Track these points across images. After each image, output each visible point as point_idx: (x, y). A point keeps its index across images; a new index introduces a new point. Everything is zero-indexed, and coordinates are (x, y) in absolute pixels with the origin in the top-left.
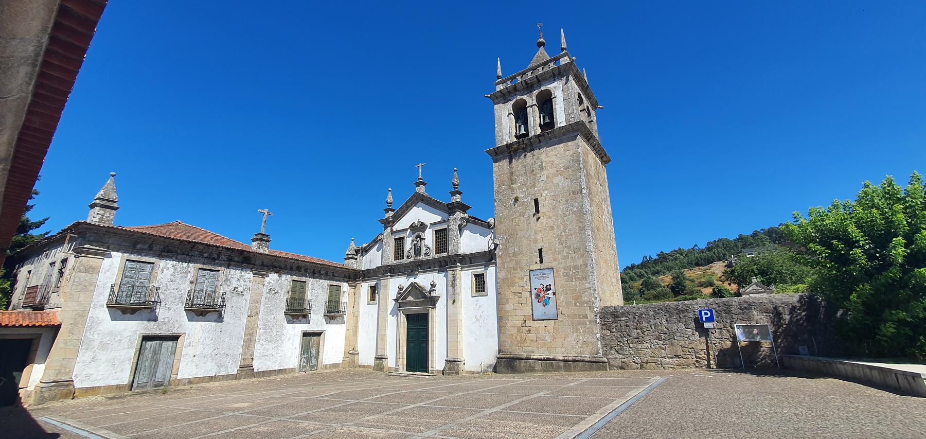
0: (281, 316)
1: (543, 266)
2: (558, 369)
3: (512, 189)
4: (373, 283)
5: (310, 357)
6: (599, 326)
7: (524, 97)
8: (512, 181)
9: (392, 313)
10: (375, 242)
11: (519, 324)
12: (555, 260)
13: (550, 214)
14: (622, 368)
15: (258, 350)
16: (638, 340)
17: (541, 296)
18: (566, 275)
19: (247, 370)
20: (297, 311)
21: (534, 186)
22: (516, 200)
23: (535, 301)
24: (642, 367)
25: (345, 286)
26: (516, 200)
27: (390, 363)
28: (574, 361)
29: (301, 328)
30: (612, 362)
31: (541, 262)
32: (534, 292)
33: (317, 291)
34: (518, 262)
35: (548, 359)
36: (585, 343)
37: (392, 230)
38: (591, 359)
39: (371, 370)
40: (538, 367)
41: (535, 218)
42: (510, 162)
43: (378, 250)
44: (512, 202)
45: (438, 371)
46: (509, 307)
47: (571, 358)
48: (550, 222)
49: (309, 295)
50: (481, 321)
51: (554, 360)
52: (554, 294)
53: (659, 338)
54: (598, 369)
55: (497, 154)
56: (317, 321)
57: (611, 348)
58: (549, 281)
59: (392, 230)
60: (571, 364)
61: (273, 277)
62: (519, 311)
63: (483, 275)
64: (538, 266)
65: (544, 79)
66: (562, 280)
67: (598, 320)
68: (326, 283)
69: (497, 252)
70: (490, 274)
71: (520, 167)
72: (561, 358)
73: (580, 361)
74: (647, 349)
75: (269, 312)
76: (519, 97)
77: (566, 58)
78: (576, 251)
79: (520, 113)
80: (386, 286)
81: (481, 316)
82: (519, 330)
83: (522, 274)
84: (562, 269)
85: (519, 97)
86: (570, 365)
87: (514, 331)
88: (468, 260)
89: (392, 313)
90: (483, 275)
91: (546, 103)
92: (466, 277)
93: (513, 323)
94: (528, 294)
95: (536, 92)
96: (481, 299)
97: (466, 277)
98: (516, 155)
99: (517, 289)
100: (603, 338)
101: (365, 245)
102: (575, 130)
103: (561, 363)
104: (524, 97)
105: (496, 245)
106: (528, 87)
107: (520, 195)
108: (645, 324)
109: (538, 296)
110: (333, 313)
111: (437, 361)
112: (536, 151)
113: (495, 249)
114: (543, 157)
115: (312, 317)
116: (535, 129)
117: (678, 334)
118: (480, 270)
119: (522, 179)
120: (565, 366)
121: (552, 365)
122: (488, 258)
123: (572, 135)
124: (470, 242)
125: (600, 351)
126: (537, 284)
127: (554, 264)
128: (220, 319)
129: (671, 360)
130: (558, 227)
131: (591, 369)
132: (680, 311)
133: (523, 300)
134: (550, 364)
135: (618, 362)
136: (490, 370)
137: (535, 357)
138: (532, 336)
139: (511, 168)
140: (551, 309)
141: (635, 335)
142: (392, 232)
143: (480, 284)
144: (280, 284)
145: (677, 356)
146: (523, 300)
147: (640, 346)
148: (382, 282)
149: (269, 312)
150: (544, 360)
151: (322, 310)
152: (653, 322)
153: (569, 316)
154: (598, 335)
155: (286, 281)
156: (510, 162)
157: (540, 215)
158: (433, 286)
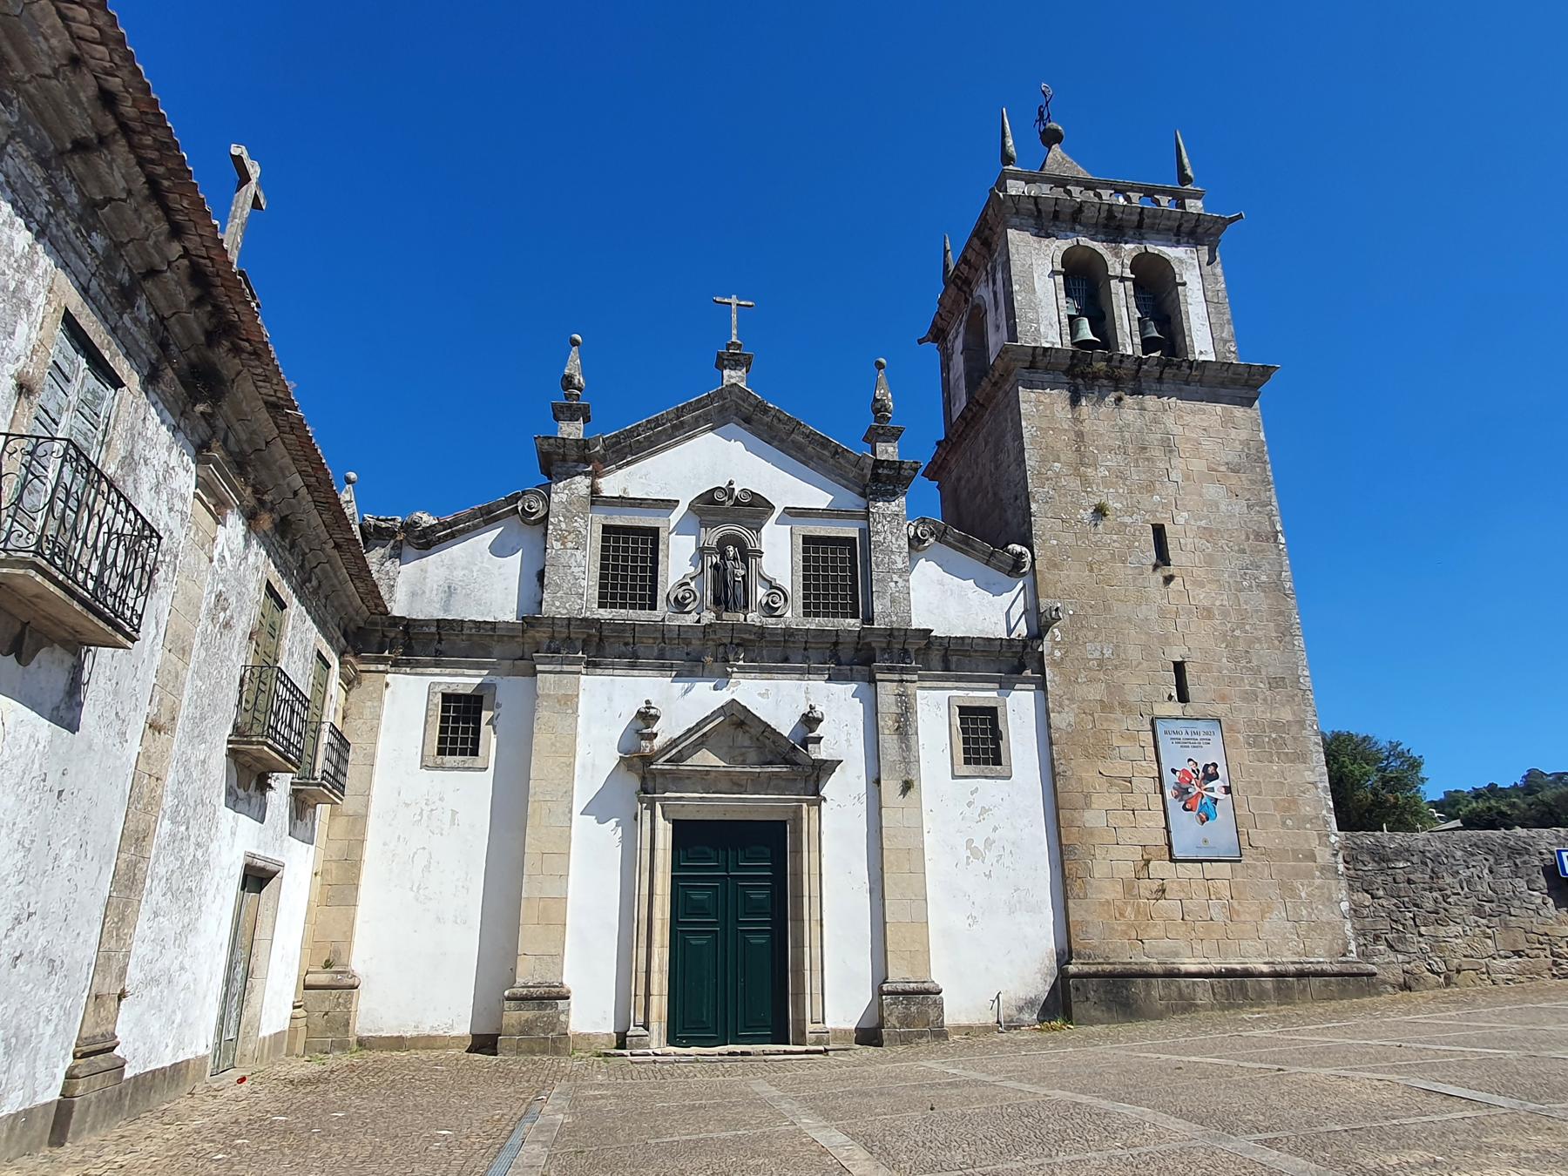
1: (1190, 710)
2: (1260, 998)
3: (1085, 481)
4: (466, 681)
6: (1344, 883)
7: (1099, 247)
8: (1082, 460)
9: (599, 808)
10: (488, 517)
11: (1126, 870)
12: (1223, 698)
13: (1200, 573)
14: (1406, 987)
16: (1440, 917)
17: (1192, 791)
18: (1254, 742)
21: (1150, 488)
22: (1100, 512)
23: (1175, 806)
24: (1448, 981)
26: (1100, 512)
27: (591, 1011)
28: (1301, 974)
30: (1382, 975)
31: (1183, 697)
32: (1170, 780)
34: (1114, 689)
35: (1231, 973)
36: (1316, 926)
37: (594, 491)
38: (1336, 968)
39: (459, 1052)
40: (1203, 996)
41: (1159, 576)
42: (1075, 402)
43: (498, 549)
44: (1087, 515)
45: (840, 1034)
46: (1093, 818)
47: (1292, 968)
48: (1201, 596)
50: (991, 856)
51: (1247, 974)
52: (1228, 790)
53: (1479, 911)
54: (1361, 993)
55: (1032, 366)
57: (1377, 938)
58: (1211, 753)
59: (594, 491)
60: (1291, 983)
62: (1120, 829)
63: (992, 712)
64: (1175, 709)
65: (1152, 227)
66: (1243, 755)
67: (1341, 867)
69: (1046, 646)
70: (1019, 711)
71: (1103, 427)
72: (1266, 969)
73: (1316, 974)
74: (1458, 937)
76: (1084, 241)
77: (1200, 204)
78: (1275, 683)
79: (1083, 281)
80: (569, 702)
81: (989, 843)
82: (1129, 888)
83: (1130, 723)
84: (1241, 727)
85: (1084, 241)
86: (1290, 988)
87: (1113, 892)
88: (935, 656)
89: (599, 808)
90: (992, 712)
91: (1156, 290)
92: (935, 710)
93: (1109, 867)
94: (1150, 786)
95: (1130, 249)
96: (988, 789)
97: (935, 710)
98: (1090, 388)
99: (1119, 768)
100: (1356, 911)
101: (427, 520)
102: (1233, 383)
103: (1268, 983)
104: (1099, 247)
105: (1040, 625)
106: (1114, 228)
107: (1113, 504)
108: (1449, 880)
109: (1182, 792)
111: (838, 990)
112: (1150, 401)
113: (1038, 634)
114: (1169, 420)
116: (1128, 343)
117: (1517, 903)
118: (983, 696)
119: (1112, 460)
120: (1278, 989)
121: (1243, 991)
122: (1016, 660)
123: (1243, 393)
124: (942, 597)
125: (1353, 947)
126: (1176, 758)
127: (1220, 709)
129: (1505, 962)
130: (1225, 614)
131: (1343, 994)
132: (1514, 852)
133: (1137, 800)
134: (1236, 985)
135: (1395, 974)
136: (1030, 1017)
137: (1193, 968)
138: (1169, 905)
139: (1077, 420)
140: (1220, 833)
141: (1429, 905)
142: (596, 498)
143: (981, 740)
145: (1518, 953)
146: (1137, 800)
147: (1441, 932)
148: (547, 682)
150: (1219, 975)
152: (1465, 874)
153: (1267, 853)
154: (1345, 906)
156: (1075, 402)
157: (1172, 570)
158: (810, 721)
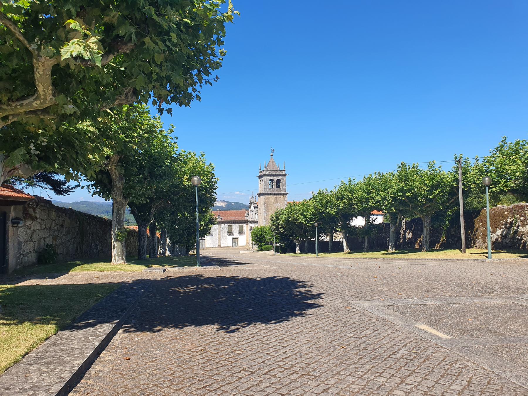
0: (226, 234)
5: (235, 244)
15: (221, 242)
19: (219, 246)
20: (230, 233)
25: (244, 225)
29: (232, 237)
33: (235, 228)
49: (233, 229)
56: (236, 235)
61: (223, 225)
68: (238, 225)
75: (223, 233)
110: (241, 232)
115: (234, 234)
128: (212, 236)
144: (225, 227)
149: (223, 233)
151: (237, 232)
155: (226, 225)
